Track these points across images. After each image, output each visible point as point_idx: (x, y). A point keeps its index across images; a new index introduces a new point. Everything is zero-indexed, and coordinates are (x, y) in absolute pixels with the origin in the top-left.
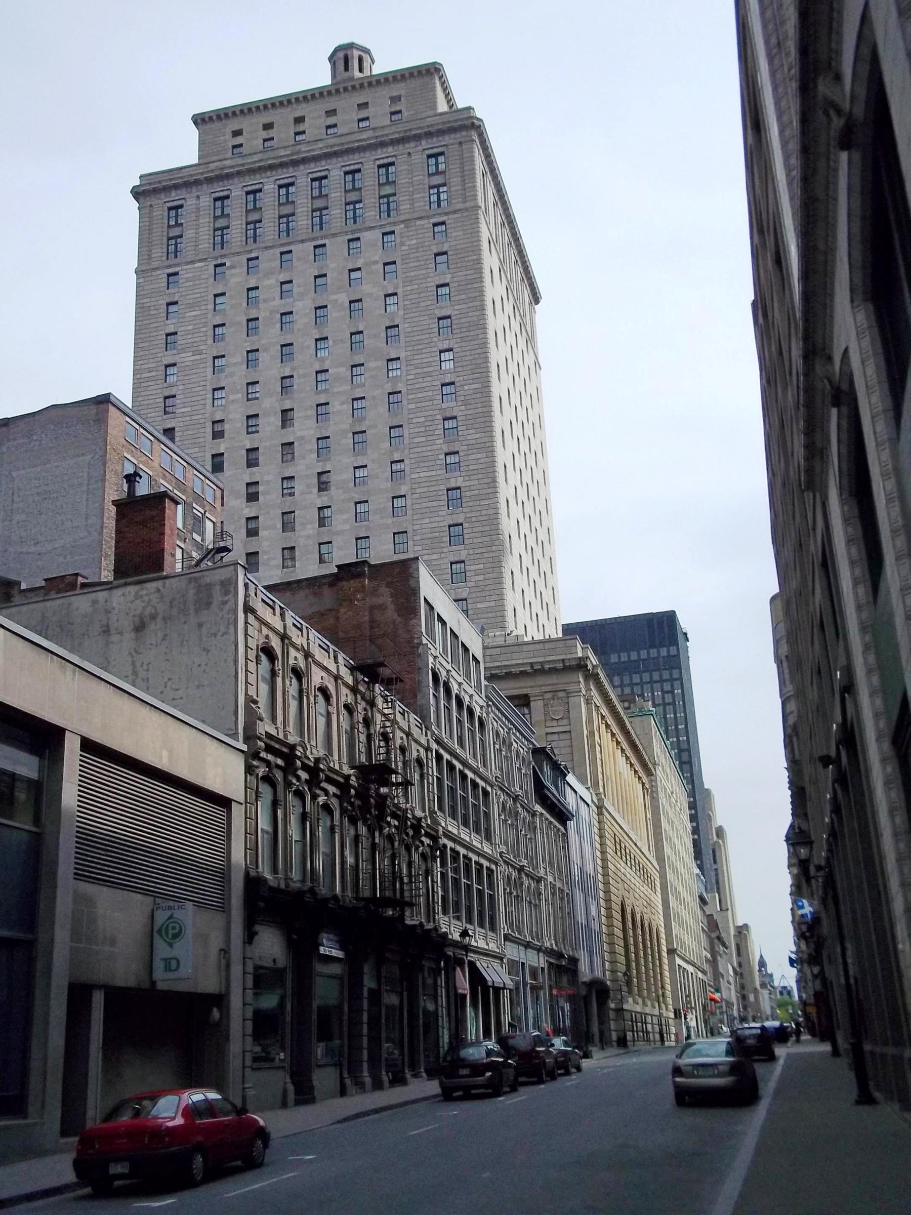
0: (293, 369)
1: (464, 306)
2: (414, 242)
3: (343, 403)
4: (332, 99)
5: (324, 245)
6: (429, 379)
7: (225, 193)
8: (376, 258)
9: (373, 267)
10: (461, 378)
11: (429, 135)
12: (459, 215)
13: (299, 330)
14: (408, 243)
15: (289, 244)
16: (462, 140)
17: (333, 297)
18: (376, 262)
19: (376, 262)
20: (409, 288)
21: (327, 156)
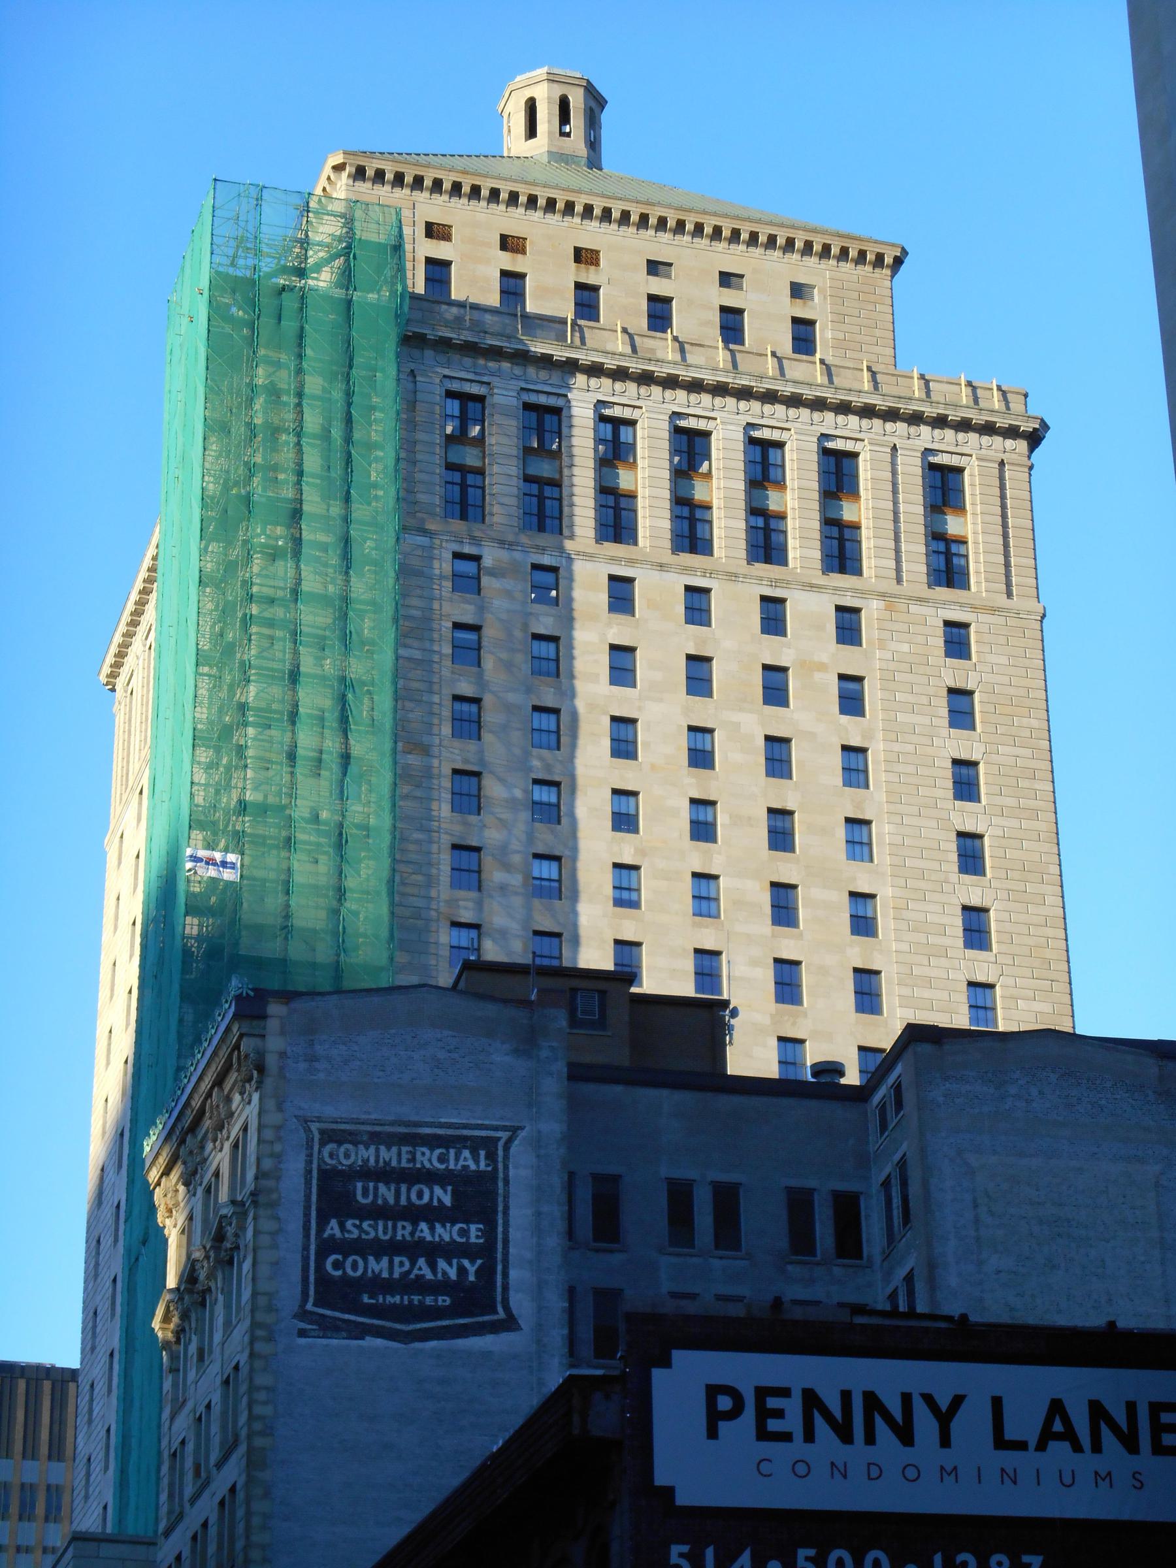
0: (642, 852)
1: (1014, 823)
2: (905, 648)
3: (754, 963)
4: (666, 237)
5: (707, 591)
6: (944, 962)
7: (475, 389)
8: (824, 658)
9: (818, 676)
10: (1011, 981)
11: (940, 422)
12: (1002, 620)
13: (653, 767)
14: (893, 646)
15: (631, 562)
16: (1005, 457)
17: (737, 717)
18: (822, 667)
19: (822, 667)
20: (897, 747)
21: (720, 390)
